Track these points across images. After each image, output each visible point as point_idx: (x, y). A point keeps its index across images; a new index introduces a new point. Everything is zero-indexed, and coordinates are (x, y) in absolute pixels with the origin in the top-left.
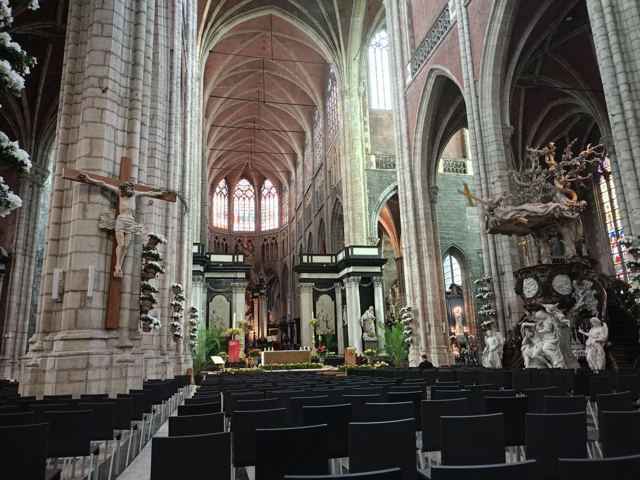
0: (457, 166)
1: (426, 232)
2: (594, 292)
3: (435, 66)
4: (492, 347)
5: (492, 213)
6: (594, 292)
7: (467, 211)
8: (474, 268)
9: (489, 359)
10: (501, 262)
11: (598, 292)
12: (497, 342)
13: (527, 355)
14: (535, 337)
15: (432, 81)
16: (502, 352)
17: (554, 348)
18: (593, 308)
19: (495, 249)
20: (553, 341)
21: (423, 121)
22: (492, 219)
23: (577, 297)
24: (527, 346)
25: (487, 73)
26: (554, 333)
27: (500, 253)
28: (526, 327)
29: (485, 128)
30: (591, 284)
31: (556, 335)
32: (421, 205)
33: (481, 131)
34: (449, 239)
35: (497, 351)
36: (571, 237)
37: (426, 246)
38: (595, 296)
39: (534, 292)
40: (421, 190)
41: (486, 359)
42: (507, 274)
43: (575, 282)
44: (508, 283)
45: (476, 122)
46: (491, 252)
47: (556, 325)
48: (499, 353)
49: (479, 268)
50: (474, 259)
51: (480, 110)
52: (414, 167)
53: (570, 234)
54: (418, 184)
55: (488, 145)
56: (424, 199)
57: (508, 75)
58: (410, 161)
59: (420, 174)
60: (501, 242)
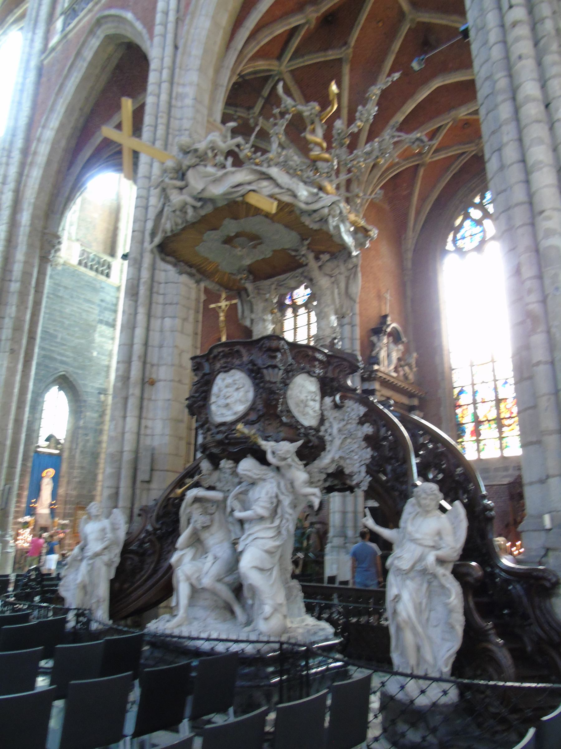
0: (98, 263)
1: (18, 306)
2: (368, 429)
3: (107, 13)
4: (94, 547)
5: (179, 183)
6: (368, 429)
7: (98, 330)
8: (88, 414)
9: (80, 578)
10: (153, 357)
11: (377, 431)
12: (109, 535)
13: (188, 578)
14: (214, 528)
15: (95, 43)
16: (117, 560)
17: (268, 566)
18: (355, 469)
19: (148, 329)
20: (271, 544)
21: (63, 110)
22: (176, 198)
23: (327, 438)
24: (188, 554)
25: (204, 12)
26: (277, 522)
27: (155, 338)
28: (197, 500)
29: (179, 104)
30: (362, 410)
31: (279, 527)
32: (20, 255)
33: (170, 106)
34: (62, 362)
35: (105, 558)
36: (333, 300)
37: (10, 331)
38: (367, 438)
39: (241, 408)
40: (27, 229)
41: (71, 577)
42: (160, 385)
43: (328, 400)
44: (160, 404)
45: (165, 86)
46: (139, 332)
47: (286, 501)
48: (108, 565)
49: (96, 415)
50: (92, 400)
51: (177, 70)
52: (25, 186)
53: (333, 293)
54: (25, 218)
55: (177, 133)
56: (30, 246)
57: (233, 44)
58: (20, 174)
59: (33, 201)
60: (163, 318)
